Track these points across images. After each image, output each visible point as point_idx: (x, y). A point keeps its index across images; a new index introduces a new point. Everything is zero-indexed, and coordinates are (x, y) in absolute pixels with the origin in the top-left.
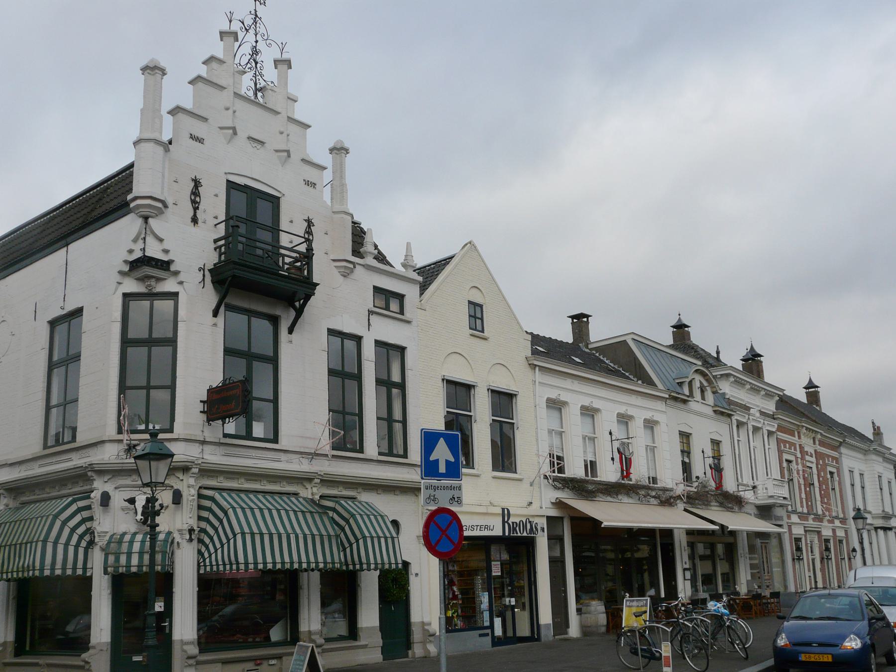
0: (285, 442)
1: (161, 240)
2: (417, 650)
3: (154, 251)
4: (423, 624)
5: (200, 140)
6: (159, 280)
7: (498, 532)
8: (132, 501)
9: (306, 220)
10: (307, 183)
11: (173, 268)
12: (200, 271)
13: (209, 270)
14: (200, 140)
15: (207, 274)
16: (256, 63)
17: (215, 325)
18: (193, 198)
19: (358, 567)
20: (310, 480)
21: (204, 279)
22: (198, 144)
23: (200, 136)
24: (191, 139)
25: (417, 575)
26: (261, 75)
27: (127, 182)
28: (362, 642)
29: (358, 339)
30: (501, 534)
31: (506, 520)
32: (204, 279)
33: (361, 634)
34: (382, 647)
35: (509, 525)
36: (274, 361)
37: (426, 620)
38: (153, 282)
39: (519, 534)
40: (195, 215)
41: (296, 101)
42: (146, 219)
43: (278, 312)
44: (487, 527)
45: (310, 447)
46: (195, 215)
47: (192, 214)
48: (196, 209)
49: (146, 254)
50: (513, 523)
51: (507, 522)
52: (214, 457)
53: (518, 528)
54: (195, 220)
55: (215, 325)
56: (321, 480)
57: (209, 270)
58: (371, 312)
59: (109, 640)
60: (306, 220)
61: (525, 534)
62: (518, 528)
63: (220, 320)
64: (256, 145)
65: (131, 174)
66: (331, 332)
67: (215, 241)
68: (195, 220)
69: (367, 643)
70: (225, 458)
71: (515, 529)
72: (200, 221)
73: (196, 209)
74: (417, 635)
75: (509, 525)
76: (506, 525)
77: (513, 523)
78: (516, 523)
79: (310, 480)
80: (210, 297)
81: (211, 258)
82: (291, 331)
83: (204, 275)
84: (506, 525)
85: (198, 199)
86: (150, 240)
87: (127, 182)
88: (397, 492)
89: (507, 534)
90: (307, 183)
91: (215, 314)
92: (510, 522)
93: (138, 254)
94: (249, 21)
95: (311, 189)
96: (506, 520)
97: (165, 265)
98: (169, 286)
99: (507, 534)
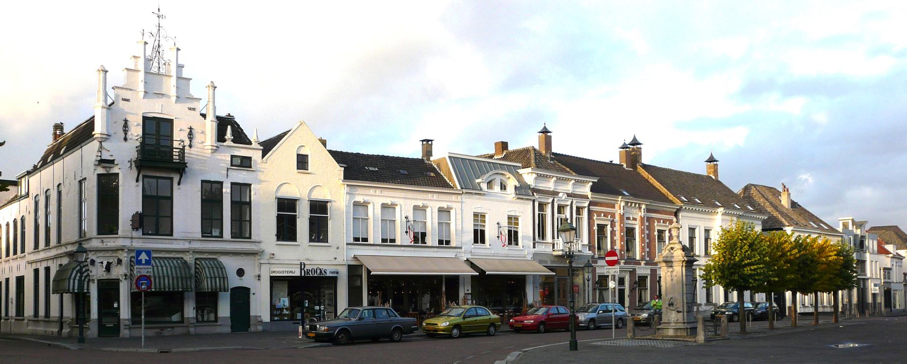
0: (175, 235)
1: (109, 151)
2: (252, 329)
3: (106, 156)
4: (256, 316)
5: (128, 100)
6: (110, 168)
7: (297, 274)
8: (102, 263)
9: (189, 128)
10: (190, 109)
11: (115, 163)
12: (129, 162)
13: (134, 161)
14: (128, 100)
15: (133, 163)
16: (159, 52)
17: (137, 186)
18: (124, 129)
19: (218, 290)
20: (188, 252)
21: (131, 166)
22: (126, 102)
23: (127, 98)
24: (122, 101)
25: (254, 294)
26: (162, 58)
27: (91, 128)
28: (219, 323)
29: (221, 183)
30: (299, 275)
31: (303, 268)
32: (131, 166)
33: (218, 320)
34: (231, 326)
35: (305, 271)
36: (171, 198)
37: (258, 315)
38: (108, 170)
39: (311, 275)
40: (125, 137)
41: (183, 67)
42: (101, 142)
43: (172, 176)
44: (291, 272)
45: (191, 236)
46: (125, 137)
47: (124, 136)
48: (126, 134)
49: (102, 158)
50: (307, 270)
51: (303, 269)
52: (138, 244)
53: (310, 273)
54: (125, 139)
55: (137, 186)
56: (193, 252)
57: (134, 161)
58: (228, 169)
59: (97, 318)
60: (189, 128)
61: (316, 275)
62: (310, 273)
63: (140, 183)
64: (159, 95)
65: (94, 120)
66: (203, 181)
67: (137, 147)
68: (125, 139)
69: (221, 324)
70: (143, 244)
71: (308, 273)
72: (128, 139)
73: (126, 134)
74: (252, 322)
75: (305, 271)
76: (303, 271)
77: (307, 270)
78: (310, 270)
79: (188, 252)
80: (134, 172)
81: (134, 155)
82: (179, 184)
83: (131, 164)
84: (303, 271)
85: (127, 129)
86: (103, 152)
87: (91, 128)
88: (242, 255)
89: (303, 275)
90: (190, 109)
91: (137, 181)
92: (305, 269)
93: (99, 158)
94: (155, 31)
95: (192, 111)
96: (303, 268)
97: (112, 162)
98: (115, 170)
99: (303, 275)
